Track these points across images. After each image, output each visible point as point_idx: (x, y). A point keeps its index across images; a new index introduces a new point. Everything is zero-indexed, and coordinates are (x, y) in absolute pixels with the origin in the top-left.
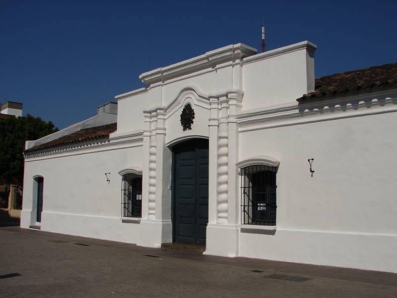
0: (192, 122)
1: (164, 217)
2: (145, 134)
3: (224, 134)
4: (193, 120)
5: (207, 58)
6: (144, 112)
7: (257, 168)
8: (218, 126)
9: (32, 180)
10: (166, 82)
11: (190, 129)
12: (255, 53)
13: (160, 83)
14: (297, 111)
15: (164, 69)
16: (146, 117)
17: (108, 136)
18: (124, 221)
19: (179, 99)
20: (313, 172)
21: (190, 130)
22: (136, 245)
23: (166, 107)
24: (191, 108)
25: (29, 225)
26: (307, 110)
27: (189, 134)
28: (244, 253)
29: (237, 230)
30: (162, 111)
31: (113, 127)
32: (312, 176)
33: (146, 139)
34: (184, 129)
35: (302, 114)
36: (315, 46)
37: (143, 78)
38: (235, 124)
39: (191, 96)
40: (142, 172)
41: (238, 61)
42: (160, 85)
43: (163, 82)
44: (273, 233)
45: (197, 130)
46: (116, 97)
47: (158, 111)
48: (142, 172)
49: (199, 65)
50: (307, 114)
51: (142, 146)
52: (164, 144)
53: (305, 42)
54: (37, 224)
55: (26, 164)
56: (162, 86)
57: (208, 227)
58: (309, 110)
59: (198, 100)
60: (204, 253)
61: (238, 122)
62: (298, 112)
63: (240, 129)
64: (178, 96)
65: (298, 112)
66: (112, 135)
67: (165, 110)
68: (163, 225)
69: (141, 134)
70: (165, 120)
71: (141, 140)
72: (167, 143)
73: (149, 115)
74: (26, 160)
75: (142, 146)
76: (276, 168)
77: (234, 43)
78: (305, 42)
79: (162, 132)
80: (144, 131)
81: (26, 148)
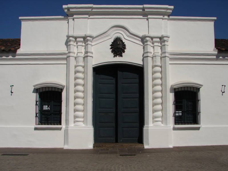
0: (124, 52)
4: (125, 50)
7: (191, 88)
8: (152, 58)
10: (91, 17)
13: (87, 16)
14: (215, 57)
18: (36, 129)
21: (121, 58)
22: (63, 148)
23: (95, 36)
24: (122, 41)
26: (221, 57)
27: (118, 59)
32: (222, 95)
33: (72, 60)
34: (114, 57)
35: (217, 58)
37: (68, 9)
43: (89, 16)
44: (198, 129)
46: (20, 18)
49: (114, 11)
50: (221, 60)
56: (88, 18)
58: (222, 57)
61: (170, 57)
62: (215, 57)
64: (108, 30)
65: (215, 57)
66: (19, 51)
70: (92, 46)
76: (198, 89)
77: (170, 5)
78: (215, 18)
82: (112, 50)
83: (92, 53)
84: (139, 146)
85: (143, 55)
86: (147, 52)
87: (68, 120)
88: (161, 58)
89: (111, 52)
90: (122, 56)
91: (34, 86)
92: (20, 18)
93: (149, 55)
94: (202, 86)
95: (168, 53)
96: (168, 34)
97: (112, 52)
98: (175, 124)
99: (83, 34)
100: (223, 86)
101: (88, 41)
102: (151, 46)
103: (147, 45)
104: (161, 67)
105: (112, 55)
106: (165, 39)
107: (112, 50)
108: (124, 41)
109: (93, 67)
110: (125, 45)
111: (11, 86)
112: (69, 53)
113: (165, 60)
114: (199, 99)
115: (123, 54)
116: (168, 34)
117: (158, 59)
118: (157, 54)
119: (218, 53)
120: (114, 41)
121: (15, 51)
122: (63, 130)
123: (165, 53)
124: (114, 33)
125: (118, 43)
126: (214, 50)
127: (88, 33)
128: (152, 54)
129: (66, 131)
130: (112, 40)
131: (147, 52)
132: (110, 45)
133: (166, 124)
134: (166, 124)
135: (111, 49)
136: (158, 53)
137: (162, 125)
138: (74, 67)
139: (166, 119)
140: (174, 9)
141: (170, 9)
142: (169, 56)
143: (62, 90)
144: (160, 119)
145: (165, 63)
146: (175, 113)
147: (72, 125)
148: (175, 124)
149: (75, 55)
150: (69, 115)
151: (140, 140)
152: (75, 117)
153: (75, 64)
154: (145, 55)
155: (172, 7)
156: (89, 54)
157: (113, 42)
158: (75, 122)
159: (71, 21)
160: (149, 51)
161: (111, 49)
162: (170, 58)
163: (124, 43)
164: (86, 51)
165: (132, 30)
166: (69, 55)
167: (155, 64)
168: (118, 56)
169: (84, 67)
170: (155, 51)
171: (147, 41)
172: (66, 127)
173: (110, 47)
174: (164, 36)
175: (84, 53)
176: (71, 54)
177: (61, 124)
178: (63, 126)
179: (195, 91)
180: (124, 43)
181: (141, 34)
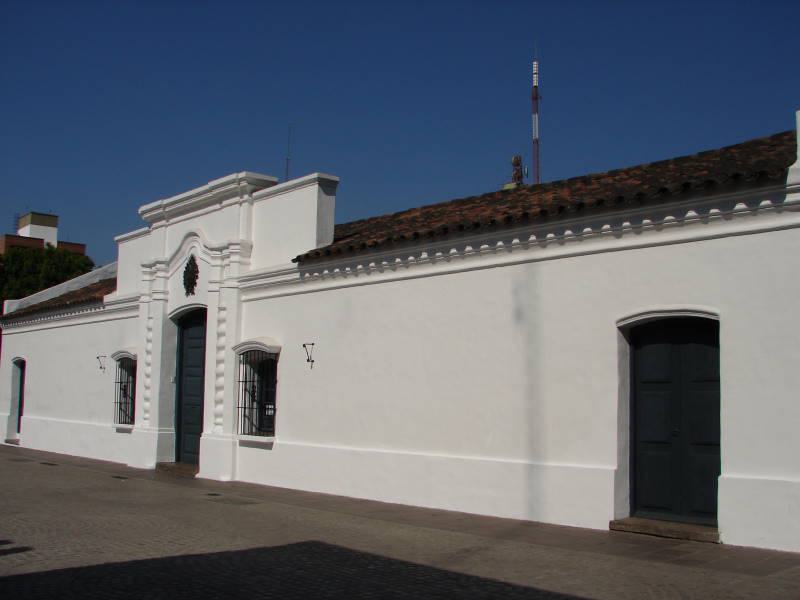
1: (161, 423)
2: (143, 299)
3: (223, 305)
5: (210, 190)
6: (143, 266)
9: (12, 364)
10: (171, 221)
11: (193, 293)
12: (275, 184)
13: (163, 222)
14: (297, 275)
15: (166, 202)
16: (145, 273)
17: (101, 300)
19: (184, 248)
20: (308, 361)
22: (125, 465)
23: (167, 256)
25: (5, 438)
28: (241, 476)
29: (234, 444)
30: (163, 266)
31: (110, 285)
35: (302, 280)
36: (336, 179)
38: (236, 290)
39: (196, 245)
40: (135, 356)
41: (246, 197)
42: (162, 226)
44: (268, 446)
45: (197, 299)
46: (117, 238)
47: (158, 266)
48: (135, 356)
51: (137, 316)
52: (164, 315)
53: (315, 175)
54: (18, 436)
55: (4, 337)
56: (166, 226)
57: (203, 438)
59: (204, 252)
60: (197, 476)
63: (244, 298)
66: (107, 298)
67: (168, 263)
68: (160, 436)
69: (136, 299)
70: (167, 278)
71: (136, 308)
72: (169, 312)
73: (148, 270)
74: (4, 332)
75: (137, 316)
78: (315, 175)
79: (161, 296)
80: (143, 295)
81: (5, 312)
84: (706, 533)
115: (196, 289)
151: (707, 512)
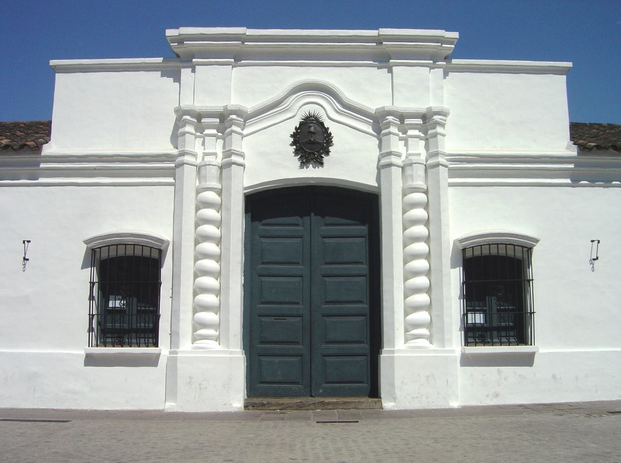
0: (327, 153)
8: (403, 168)
24: (322, 124)
27: (312, 173)
33: (189, 174)
34: (302, 167)
37: (181, 40)
46: (53, 62)
62: (573, 166)
65: (573, 166)
70: (243, 136)
78: (570, 64)
82: (295, 147)
83: (242, 155)
85: (379, 160)
86: (390, 154)
87: (177, 334)
88: (426, 168)
89: (294, 154)
90: (321, 164)
91: (87, 242)
92: (53, 62)
93: (394, 159)
94: (537, 241)
95: (444, 155)
96: (445, 106)
97: (296, 152)
98: (467, 343)
99: (216, 105)
100: (592, 241)
101: (232, 122)
102: (401, 139)
103: (390, 133)
104: (426, 192)
105: (296, 161)
106: (437, 118)
107: (295, 147)
108: (327, 124)
109: (245, 193)
110: (330, 134)
111: (24, 242)
112: (183, 154)
113: (438, 173)
114: (531, 279)
115: (326, 159)
116: (445, 106)
117: (420, 171)
118: (414, 159)
119: (578, 153)
120: (301, 124)
121: (38, 148)
122: (163, 361)
123: (436, 154)
124: (301, 103)
125: (312, 129)
126: (567, 148)
127: (234, 101)
128: (403, 158)
129: (173, 363)
130: (296, 122)
131: (390, 154)
132: (292, 136)
133: (442, 342)
134: (442, 342)
135: (292, 145)
136: (419, 154)
137: (432, 347)
138: (194, 194)
139: (442, 331)
140: (459, 40)
141: (449, 41)
142: (447, 163)
143: (161, 253)
144: (424, 331)
145: (438, 182)
146: (465, 315)
147: (186, 345)
148: (467, 343)
149: (199, 161)
150: (178, 320)
152: (198, 325)
153: (197, 184)
154: (384, 161)
155: (455, 35)
156: (234, 158)
157: (298, 126)
158: (194, 340)
159: (186, 73)
160: (393, 149)
161: (293, 144)
162: (450, 169)
163: (328, 128)
164: (227, 149)
165: (350, 96)
166: (180, 159)
167: (410, 184)
168: (311, 166)
169: (220, 192)
170: (410, 148)
171: (388, 125)
172: (170, 353)
173: (292, 140)
174: (434, 110)
175: (220, 155)
176: (187, 158)
177: (156, 344)
178: (164, 348)
179: (519, 254)
180: (328, 128)
181: (372, 105)
